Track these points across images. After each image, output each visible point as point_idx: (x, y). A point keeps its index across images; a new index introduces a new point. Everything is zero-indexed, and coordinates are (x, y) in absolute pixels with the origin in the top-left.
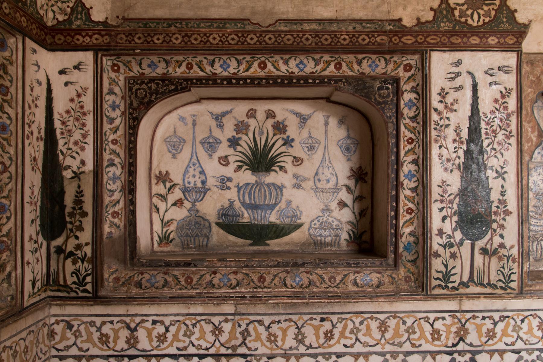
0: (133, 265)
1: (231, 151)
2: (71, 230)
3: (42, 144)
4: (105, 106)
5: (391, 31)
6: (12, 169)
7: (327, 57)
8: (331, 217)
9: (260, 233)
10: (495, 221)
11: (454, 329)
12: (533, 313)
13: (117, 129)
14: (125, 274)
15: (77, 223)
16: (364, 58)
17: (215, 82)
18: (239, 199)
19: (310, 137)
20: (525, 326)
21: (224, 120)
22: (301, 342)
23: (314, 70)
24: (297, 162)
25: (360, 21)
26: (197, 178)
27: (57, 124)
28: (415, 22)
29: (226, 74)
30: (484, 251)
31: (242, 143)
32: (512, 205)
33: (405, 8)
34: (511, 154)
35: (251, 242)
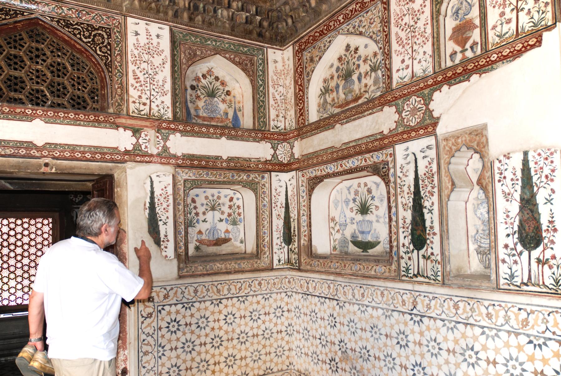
5: (380, 139)
10: (428, 239)
11: (411, 301)
12: (450, 297)
14: (308, 260)
20: (446, 304)
22: (354, 297)
29: (331, 172)
30: (424, 257)
31: (357, 200)
32: (437, 229)
34: (435, 198)
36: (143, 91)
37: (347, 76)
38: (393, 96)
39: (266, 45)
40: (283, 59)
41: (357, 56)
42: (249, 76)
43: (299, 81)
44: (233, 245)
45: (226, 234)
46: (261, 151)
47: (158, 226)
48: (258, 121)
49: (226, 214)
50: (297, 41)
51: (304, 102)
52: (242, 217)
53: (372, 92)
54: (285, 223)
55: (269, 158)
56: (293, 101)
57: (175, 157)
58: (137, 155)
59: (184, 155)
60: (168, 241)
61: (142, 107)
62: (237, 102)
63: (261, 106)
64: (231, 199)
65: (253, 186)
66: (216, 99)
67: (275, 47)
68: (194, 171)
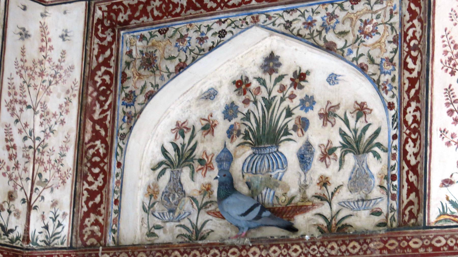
37: (266, 138)
38: (427, 242)
40: (43, 28)
41: (300, 94)
51: (107, 175)
53: (343, 204)
56: (69, 160)
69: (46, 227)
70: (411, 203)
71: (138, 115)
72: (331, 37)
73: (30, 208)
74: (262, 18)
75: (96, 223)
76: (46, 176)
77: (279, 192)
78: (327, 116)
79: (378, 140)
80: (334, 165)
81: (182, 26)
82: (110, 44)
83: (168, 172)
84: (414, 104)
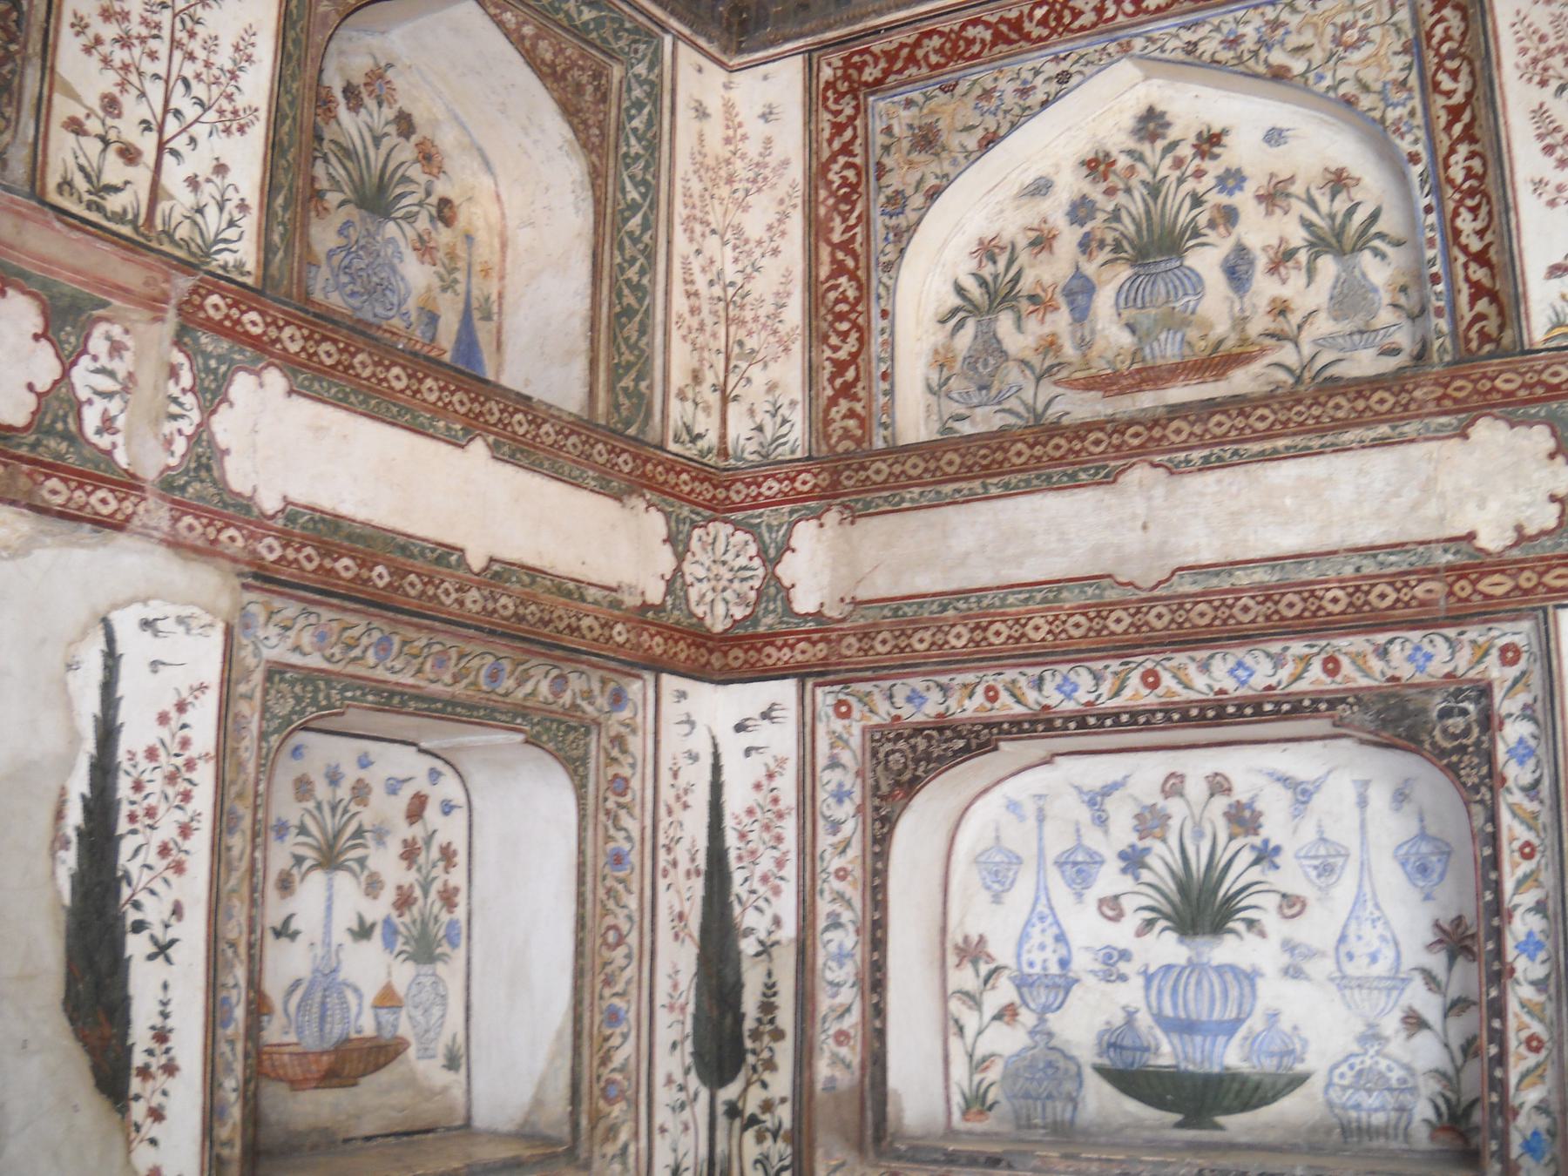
0: (880, 1154)
1: (1127, 883)
2: (754, 1069)
3: (698, 885)
4: (821, 795)
5: (1450, 568)
6: (633, 939)
7: (1298, 647)
8: (1386, 1056)
9: (1199, 1097)
13: (847, 844)
15: (766, 1055)
16: (1391, 641)
17: (1049, 726)
18: (1149, 1006)
19: (1323, 840)
21: (1111, 804)
23: (1273, 681)
24: (1291, 906)
25: (1371, 550)
26: (1048, 954)
27: (731, 840)
28: (1510, 537)
29: (1069, 706)
31: (1151, 860)
33: (1482, 505)
35: (1178, 1117)
36: (133, 78)
37: (1156, 248)
39: (673, 23)
40: (729, 107)
41: (1213, 168)
42: (586, 146)
43: (837, 223)
44: (411, 1082)
45: (386, 1016)
46: (604, 543)
47: (119, 966)
48: (611, 388)
49: (388, 895)
50: (840, 43)
52: (460, 913)
54: (704, 960)
55: (655, 594)
56: (794, 314)
57: (240, 511)
58: (54, 468)
59: (291, 513)
60: (170, 1069)
61: (114, 170)
62: (477, 268)
63: (628, 312)
64: (416, 811)
65: (563, 737)
66: (391, 229)
67: (702, 42)
68: (327, 615)
69: (760, 429)
70: (1480, 317)
71: (913, 228)
72: (1277, 57)
73: (725, 400)
74: (1139, 43)
75: (851, 414)
76: (750, 343)
77: (1192, 334)
78: (1274, 196)
79: (1381, 226)
80: (1297, 279)
81: (985, 76)
82: (852, 119)
83: (971, 325)
84: (1463, 150)
